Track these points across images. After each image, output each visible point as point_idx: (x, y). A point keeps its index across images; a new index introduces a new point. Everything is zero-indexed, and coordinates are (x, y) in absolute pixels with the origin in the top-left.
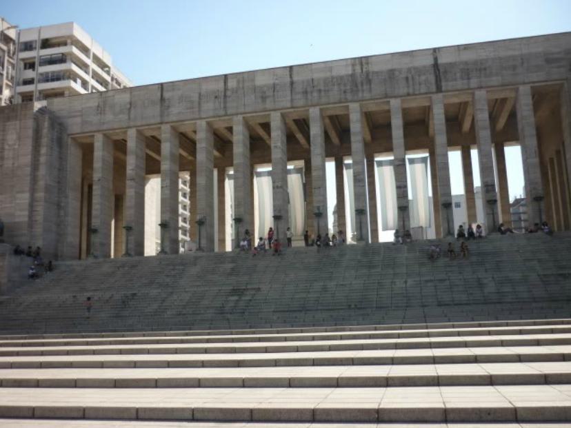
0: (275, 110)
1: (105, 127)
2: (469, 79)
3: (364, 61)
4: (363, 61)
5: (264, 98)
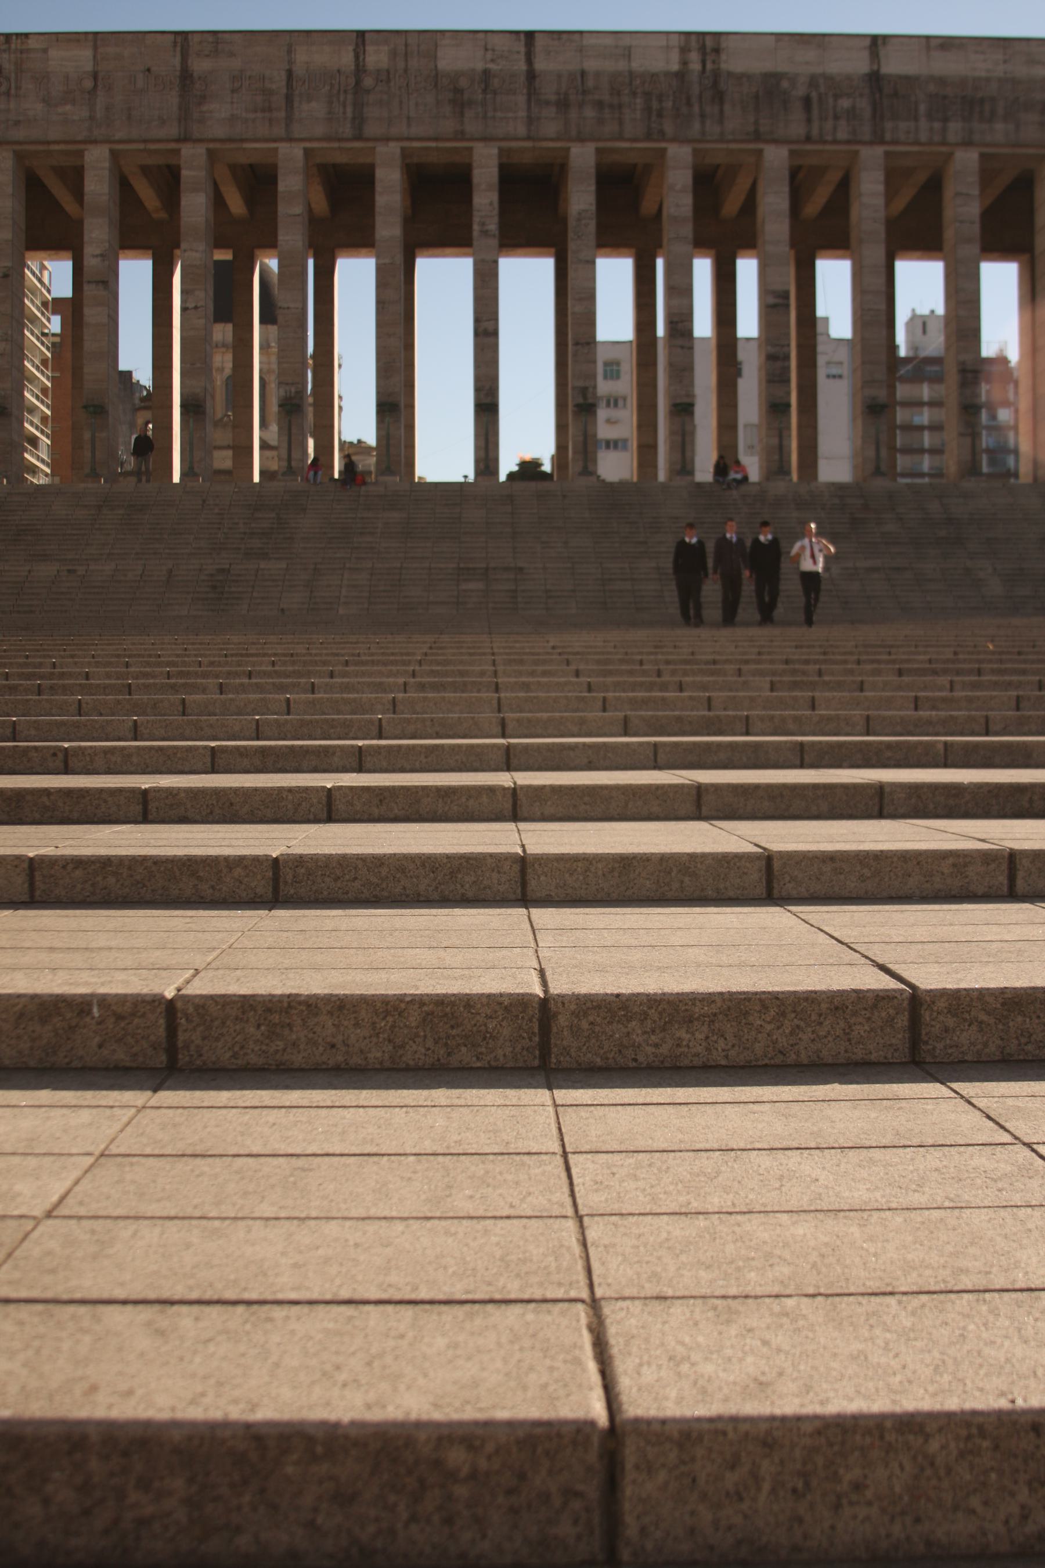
0: (485, 139)
1: (20, 134)
2: (945, 120)
3: (709, 43)
4: (707, 45)
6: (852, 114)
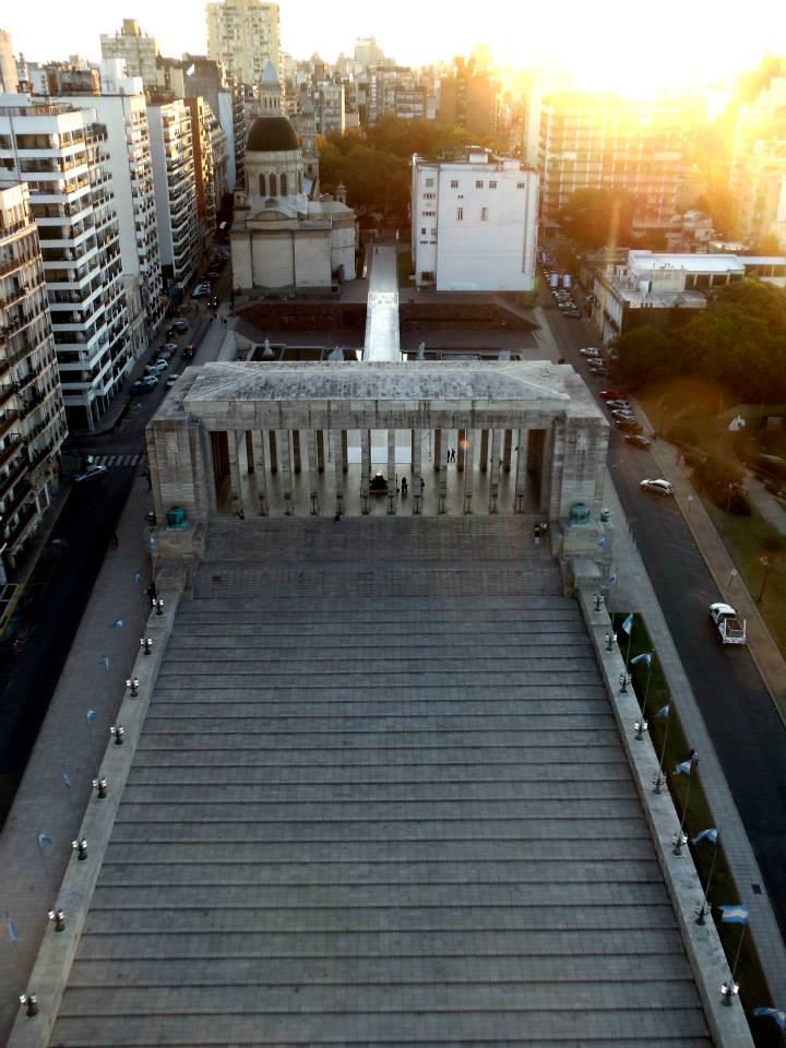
6: (466, 421)
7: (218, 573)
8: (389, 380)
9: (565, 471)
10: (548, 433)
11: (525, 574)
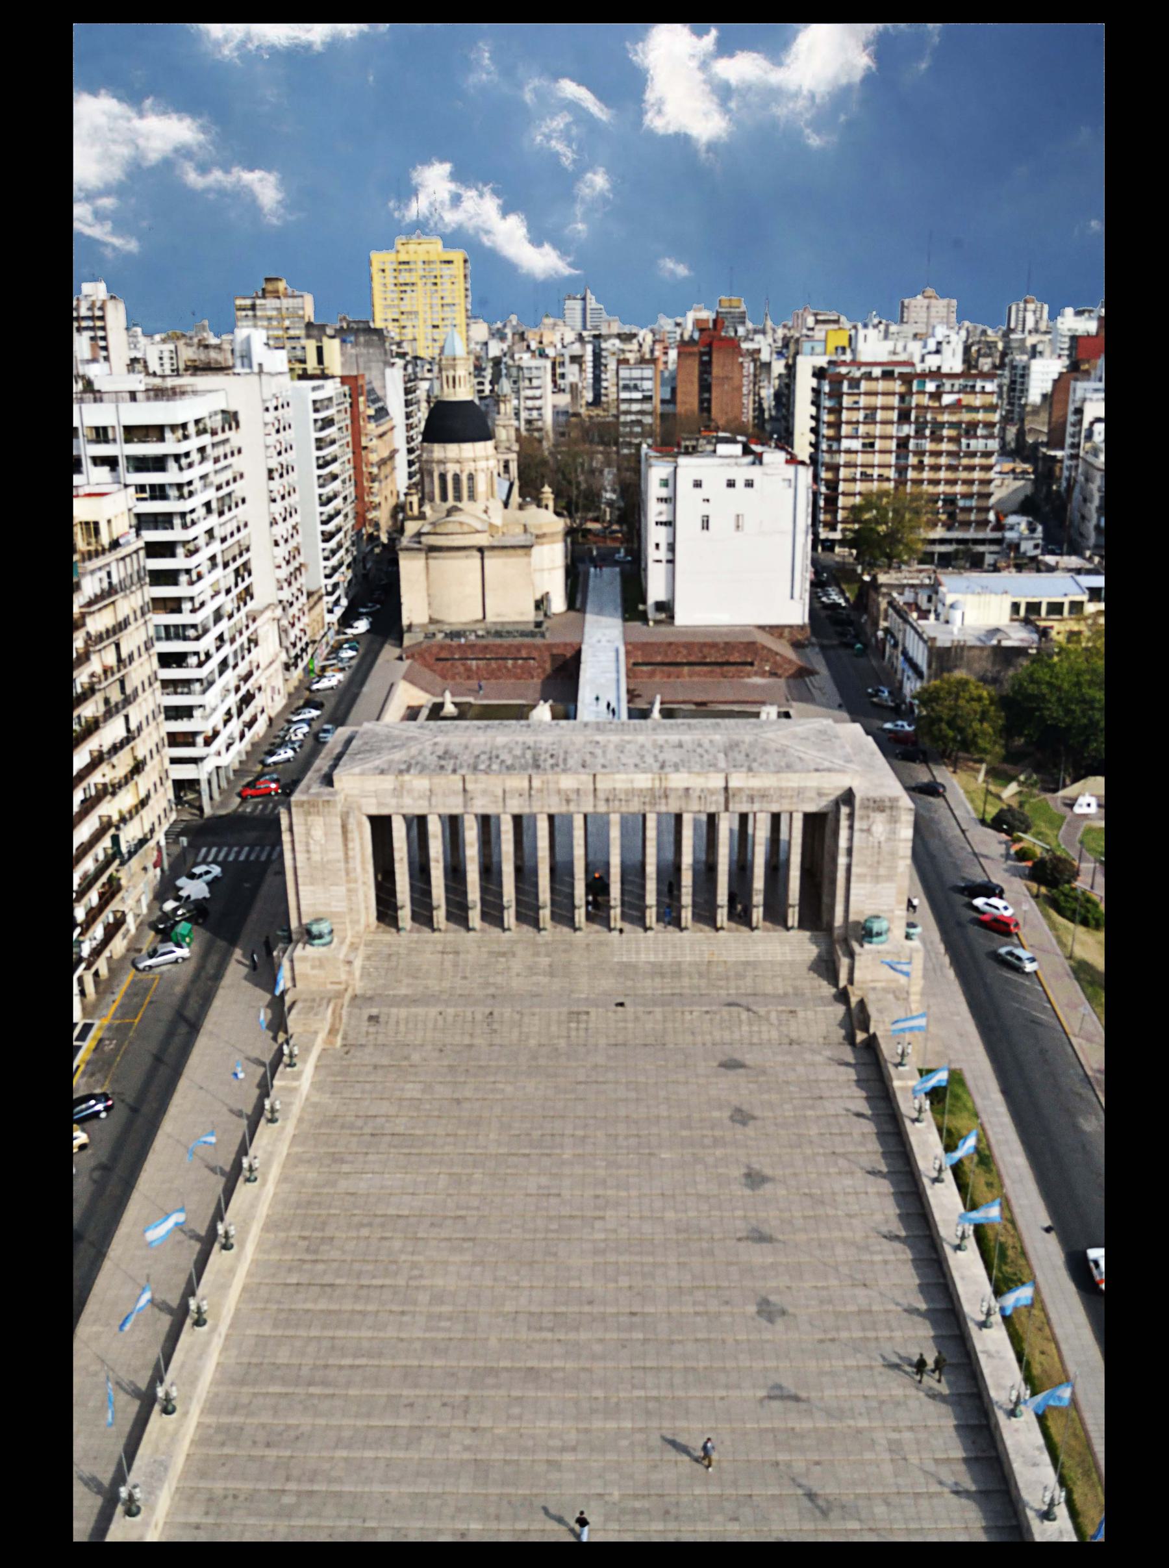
5: (568, 801)
6: (717, 802)
7: (374, 1011)
8: (612, 746)
9: (854, 870)
10: (830, 816)
11: (801, 1014)
